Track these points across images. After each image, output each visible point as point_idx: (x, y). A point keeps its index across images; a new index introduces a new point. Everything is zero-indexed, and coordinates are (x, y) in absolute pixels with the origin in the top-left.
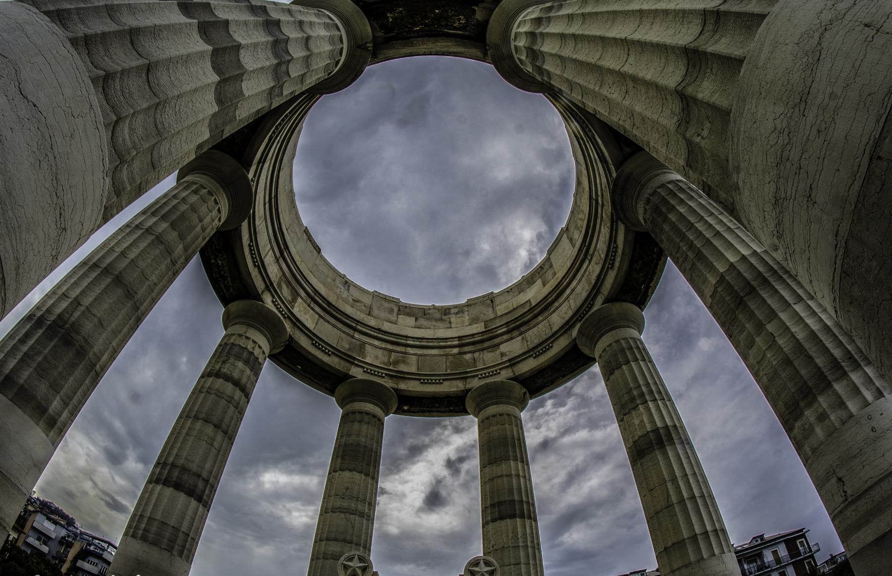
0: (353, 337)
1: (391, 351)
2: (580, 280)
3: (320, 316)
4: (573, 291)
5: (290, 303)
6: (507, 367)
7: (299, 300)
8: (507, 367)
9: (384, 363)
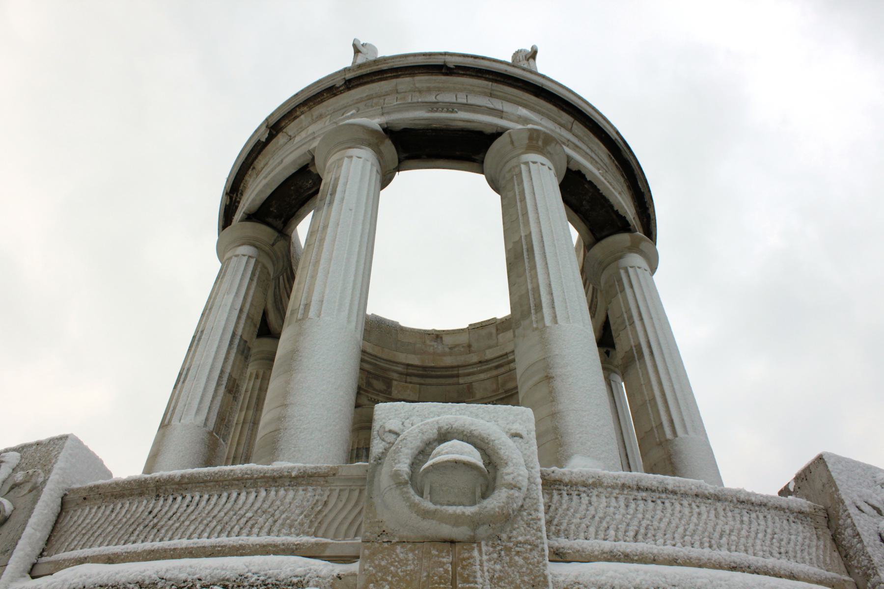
3: (420, 384)
7: (395, 383)
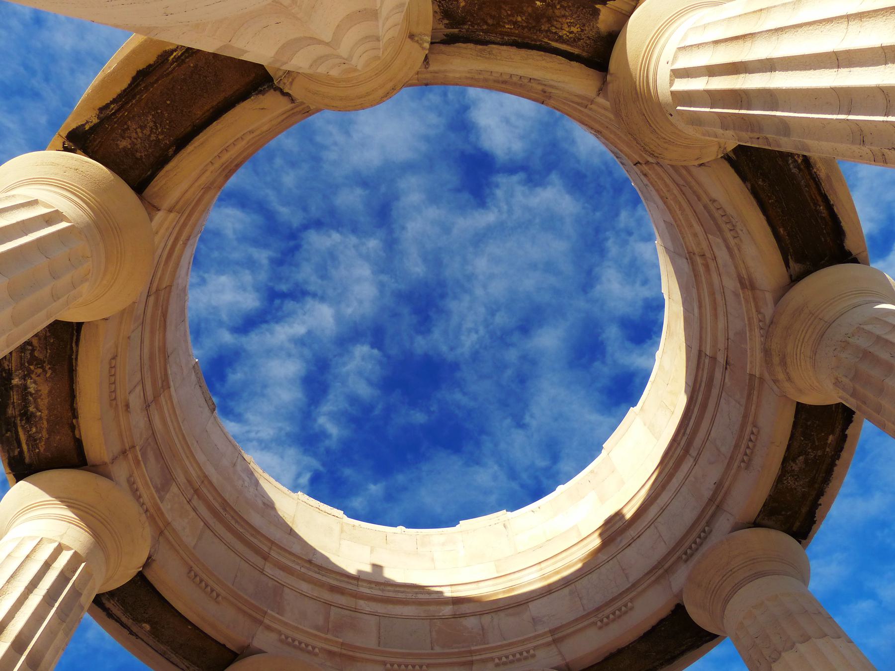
0: (262, 572)
1: (329, 604)
2: (678, 491)
3: (206, 524)
4: (663, 510)
5: (158, 491)
6: (548, 644)
7: (174, 489)
8: (548, 644)
9: (317, 628)
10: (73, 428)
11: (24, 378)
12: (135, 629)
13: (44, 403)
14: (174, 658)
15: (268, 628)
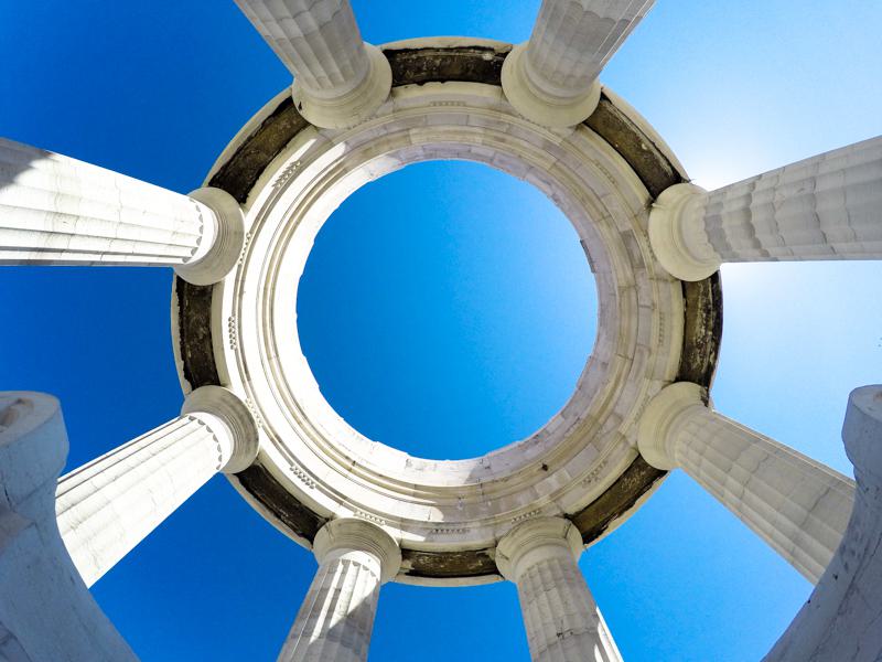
10: (686, 305)
11: (706, 335)
12: (651, 146)
13: (699, 321)
14: (626, 121)
15: (558, 135)
